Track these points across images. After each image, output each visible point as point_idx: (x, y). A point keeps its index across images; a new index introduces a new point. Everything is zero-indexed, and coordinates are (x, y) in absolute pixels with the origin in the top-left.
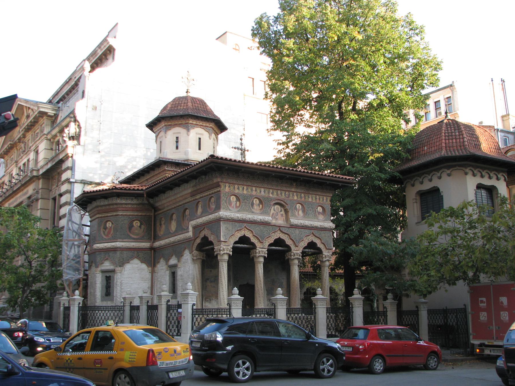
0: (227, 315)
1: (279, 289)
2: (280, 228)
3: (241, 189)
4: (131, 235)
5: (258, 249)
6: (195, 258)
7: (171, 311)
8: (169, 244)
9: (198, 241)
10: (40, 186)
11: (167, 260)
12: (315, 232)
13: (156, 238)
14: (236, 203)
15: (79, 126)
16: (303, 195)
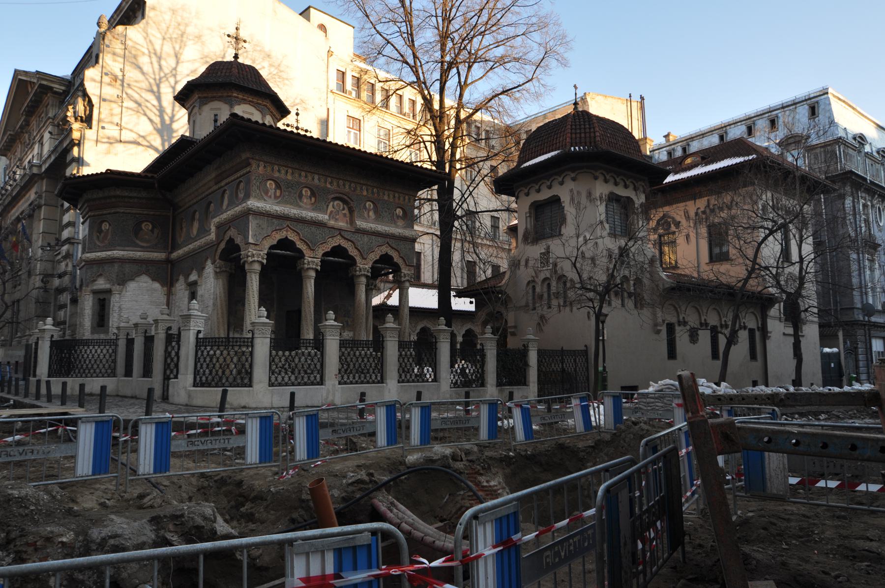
0: (248, 346)
1: (331, 312)
2: (340, 231)
3: (283, 172)
4: (138, 242)
5: (307, 259)
6: (218, 270)
7: (174, 344)
8: (189, 252)
9: (223, 245)
10: (44, 189)
11: (187, 276)
12: (391, 242)
13: (174, 248)
14: (275, 193)
15: (90, 104)
16: (375, 190)
